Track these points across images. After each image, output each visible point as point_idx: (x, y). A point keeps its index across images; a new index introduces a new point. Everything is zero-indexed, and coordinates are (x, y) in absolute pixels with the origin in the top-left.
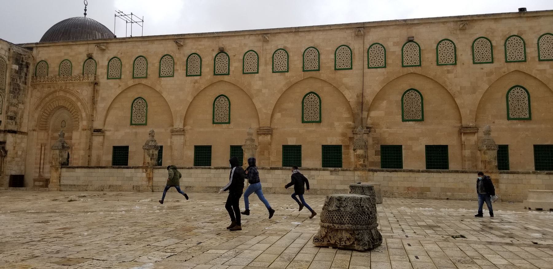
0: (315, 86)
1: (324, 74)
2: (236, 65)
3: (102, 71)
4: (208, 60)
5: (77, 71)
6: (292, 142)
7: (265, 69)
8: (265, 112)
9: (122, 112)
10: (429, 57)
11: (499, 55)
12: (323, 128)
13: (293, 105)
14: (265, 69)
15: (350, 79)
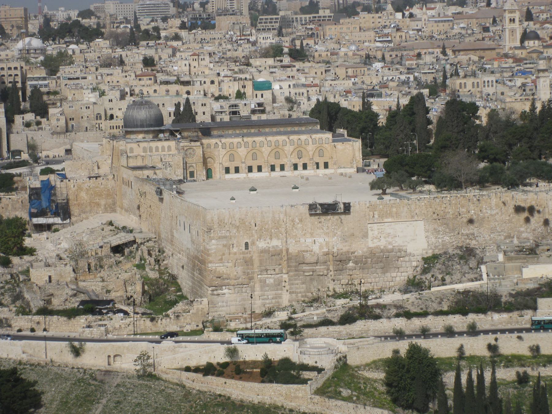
0: (278, 150)
1: (280, 147)
2: (258, 145)
3: (220, 147)
4: (250, 144)
5: (212, 147)
6: (273, 164)
7: (265, 146)
8: (266, 156)
9: (227, 157)
10: (303, 143)
11: (317, 143)
12: (280, 160)
13: (273, 154)
14: (265, 146)
15: (286, 148)
